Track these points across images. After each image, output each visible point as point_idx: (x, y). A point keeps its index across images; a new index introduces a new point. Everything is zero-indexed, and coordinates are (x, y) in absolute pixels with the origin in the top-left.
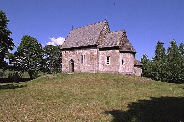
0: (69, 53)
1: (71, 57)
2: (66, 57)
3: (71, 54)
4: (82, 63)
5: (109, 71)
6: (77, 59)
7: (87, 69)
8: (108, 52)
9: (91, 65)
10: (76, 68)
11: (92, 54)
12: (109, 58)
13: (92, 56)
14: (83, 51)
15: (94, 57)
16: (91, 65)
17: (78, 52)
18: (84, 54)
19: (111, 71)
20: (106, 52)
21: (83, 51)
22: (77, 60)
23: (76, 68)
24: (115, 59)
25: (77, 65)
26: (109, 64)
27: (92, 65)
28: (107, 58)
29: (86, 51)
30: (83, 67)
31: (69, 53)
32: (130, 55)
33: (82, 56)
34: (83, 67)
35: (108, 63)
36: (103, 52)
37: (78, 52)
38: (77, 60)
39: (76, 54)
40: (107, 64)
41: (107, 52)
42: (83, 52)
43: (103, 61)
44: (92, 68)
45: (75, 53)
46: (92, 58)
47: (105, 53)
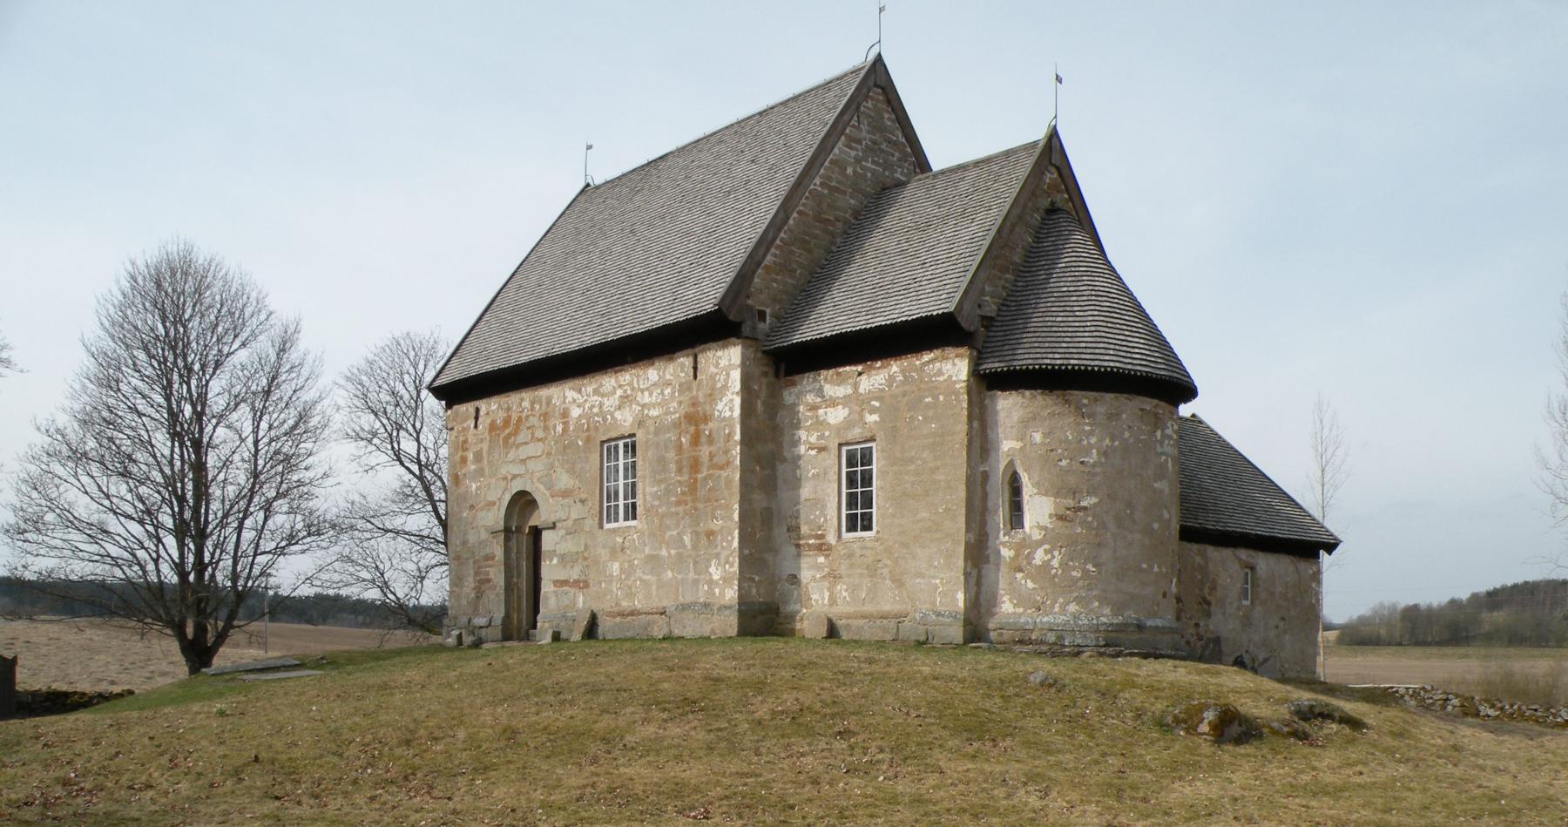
3: (521, 438)
5: (868, 608)
6: (564, 480)
8: (856, 386)
9: (687, 539)
12: (866, 458)
13: (696, 441)
15: (711, 456)
16: (687, 539)
18: (625, 419)
19: (886, 607)
21: (619, 392)
24: (935, 470)
25: (569, 546)
27: (695, 547)
29: (647, 399)
30: (616, 566)
31: (507, 422)
32: (1101, 409)
34: (615, 567)
37: (575, 412)
38: (565, 494)
39: (559, 428)
41: (849, 391)
44: (696, 582)
45: (551, 423)
46: (695, 466)
47: (833, 403)
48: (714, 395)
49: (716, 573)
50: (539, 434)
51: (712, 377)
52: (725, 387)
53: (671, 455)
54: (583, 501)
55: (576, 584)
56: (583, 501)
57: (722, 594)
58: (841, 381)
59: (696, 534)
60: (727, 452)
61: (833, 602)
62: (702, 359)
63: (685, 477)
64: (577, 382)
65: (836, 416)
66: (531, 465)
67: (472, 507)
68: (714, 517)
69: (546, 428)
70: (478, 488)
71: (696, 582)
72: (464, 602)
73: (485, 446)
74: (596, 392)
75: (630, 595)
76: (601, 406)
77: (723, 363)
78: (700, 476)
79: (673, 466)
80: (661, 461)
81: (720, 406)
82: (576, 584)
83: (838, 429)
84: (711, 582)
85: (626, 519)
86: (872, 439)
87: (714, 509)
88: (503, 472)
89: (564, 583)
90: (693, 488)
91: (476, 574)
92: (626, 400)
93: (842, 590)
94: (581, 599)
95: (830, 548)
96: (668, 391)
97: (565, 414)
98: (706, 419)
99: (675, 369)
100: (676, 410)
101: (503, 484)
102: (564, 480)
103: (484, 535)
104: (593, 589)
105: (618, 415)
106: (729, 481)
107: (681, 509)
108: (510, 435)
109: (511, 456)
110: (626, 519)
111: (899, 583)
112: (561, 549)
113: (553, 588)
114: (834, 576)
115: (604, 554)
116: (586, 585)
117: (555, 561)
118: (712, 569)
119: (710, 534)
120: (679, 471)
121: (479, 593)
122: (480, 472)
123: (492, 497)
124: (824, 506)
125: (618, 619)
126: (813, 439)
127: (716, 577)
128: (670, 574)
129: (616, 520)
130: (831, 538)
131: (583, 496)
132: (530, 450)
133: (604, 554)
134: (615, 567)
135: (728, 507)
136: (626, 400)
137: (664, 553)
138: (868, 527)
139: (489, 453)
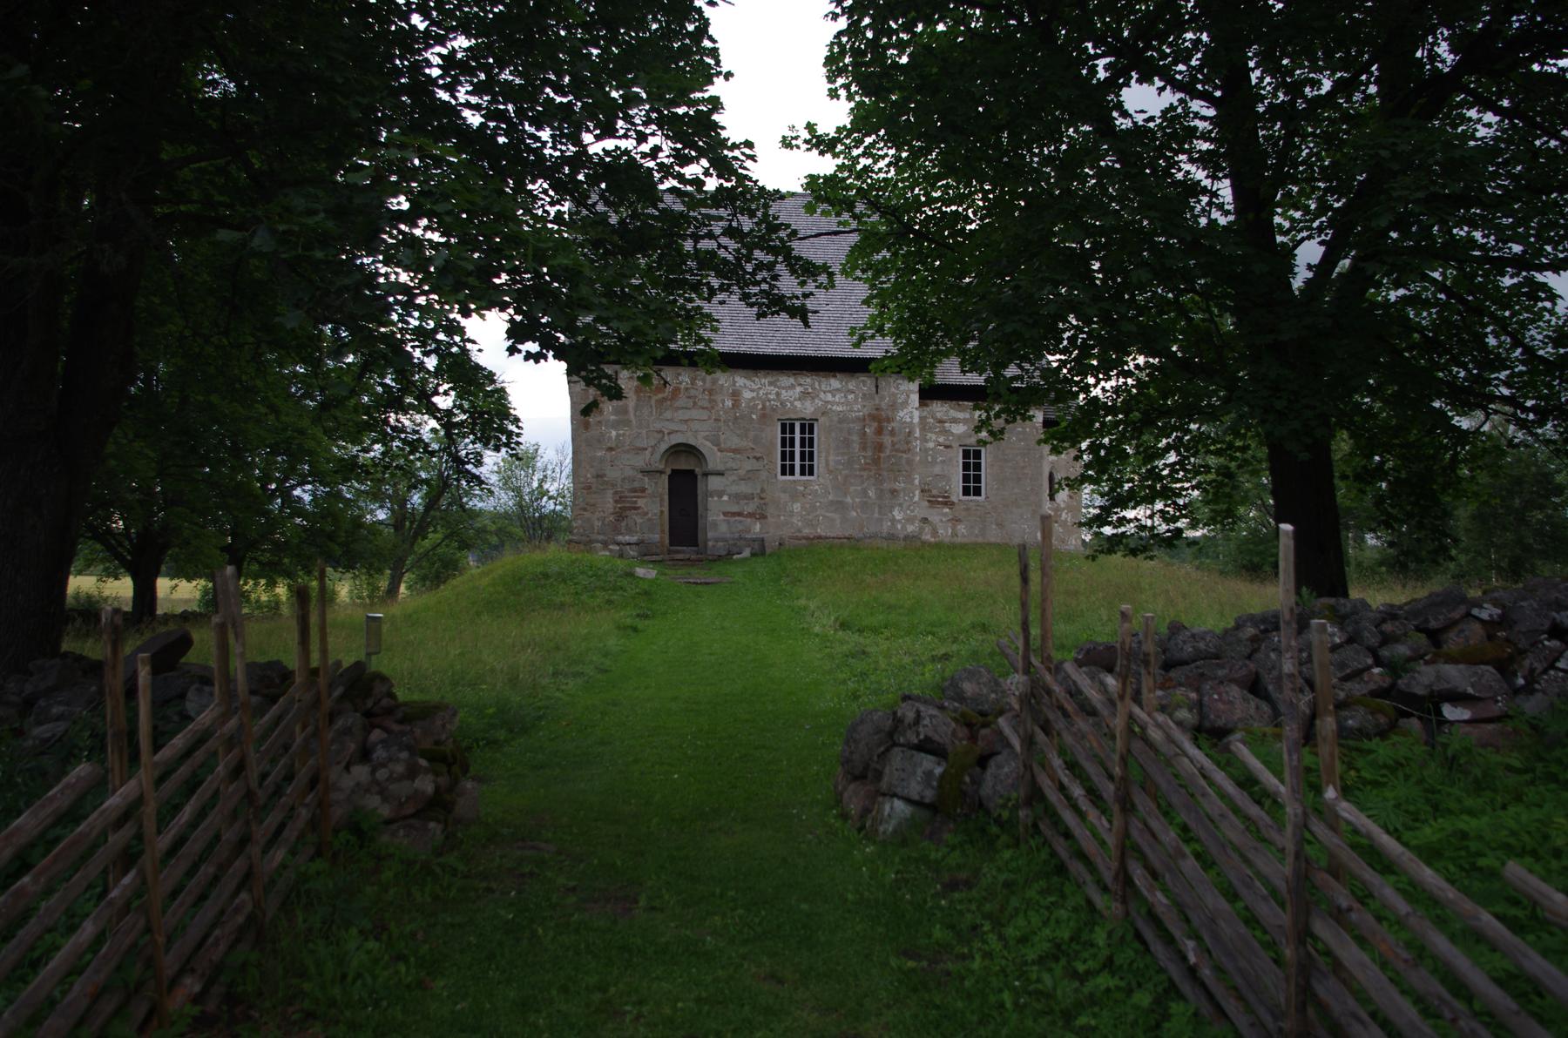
2: (627, 423)
3: (678, 403)
4: (788, 477)
5: (980, 540)
6: (735, 442)
7: (830, 525)
10: (725, 514)
11: (880, 420)
12: (978, 454)
13: (879, 431)
14: (799, 389)
15: (893, 444)
17: (751, 388)
18: (807, 409)
20: (961, 415)
21: (799, 389)
22: (735, 451)
23: (725, 514)
25: (744, 488)
26: (977, 492)
28: (966, 454)
29: (829, 397)
33: (788, 428)
34: (797, 507)
35: (972, 485)
36: (939, 415)
37: (747, 395)
38: (735, 451)
39: (729, 403)
40: (966, 492)
42: (794, 395)
43: (937, 470)
44: (880, 520)
45: (719, 398)
46: (880, 447)
47: (955, 421)
48: (894, 406)
49: (898, 514)
51: (894, 395)
52: (905, 403)
53: (855, 438)
54: (757, 459)
55: (751, 515)
56: (757, 459)
57: (904, 528)
58: (963, 411)
60: (908, 443)
61: (955, 534)
62: (882, 384)
63: (869, 454)
64: (750, 373)
65: (959, 429)
66: (695, 426)
67: (611, 449)
68: (896, 480)
69: (711, 401)
70: (618, 436)
74: (771, 384)
76: (778, 394)
77: (902, 388)
79: (856, 446)
80: (847, 443)
81: (901, 414)
82: (751, 515)
83: (959, 437)
84: (893, 520)
85: (803, 473)
88: (658, 426)
89: (739, 514)
93: (961, 528)
94: (758, 527)
95: (953, 503)
96: (851, 397)
97: (736, 395)
98: (889, 420)
99: (860, 385)
100: (859, 409)
105: (798, 404)
107: (865, 474)
108: (665, 399)
109: (668, 415)
110: (803, 473)
111: (1000, 525)
112: (734, 489)
114: (956, 520)
116: (763, 517)
117: (725, 498)
119: (894, 492)
120: (864, 449)
121: (621, 515)
122: (627, 423)
124: (949, 480)
126: (941, 440)
129: (792, 473)
130: (954, 499)
132: (695, 414)
137: (849, 500)
138: (977, 492)
139: (636, 408)
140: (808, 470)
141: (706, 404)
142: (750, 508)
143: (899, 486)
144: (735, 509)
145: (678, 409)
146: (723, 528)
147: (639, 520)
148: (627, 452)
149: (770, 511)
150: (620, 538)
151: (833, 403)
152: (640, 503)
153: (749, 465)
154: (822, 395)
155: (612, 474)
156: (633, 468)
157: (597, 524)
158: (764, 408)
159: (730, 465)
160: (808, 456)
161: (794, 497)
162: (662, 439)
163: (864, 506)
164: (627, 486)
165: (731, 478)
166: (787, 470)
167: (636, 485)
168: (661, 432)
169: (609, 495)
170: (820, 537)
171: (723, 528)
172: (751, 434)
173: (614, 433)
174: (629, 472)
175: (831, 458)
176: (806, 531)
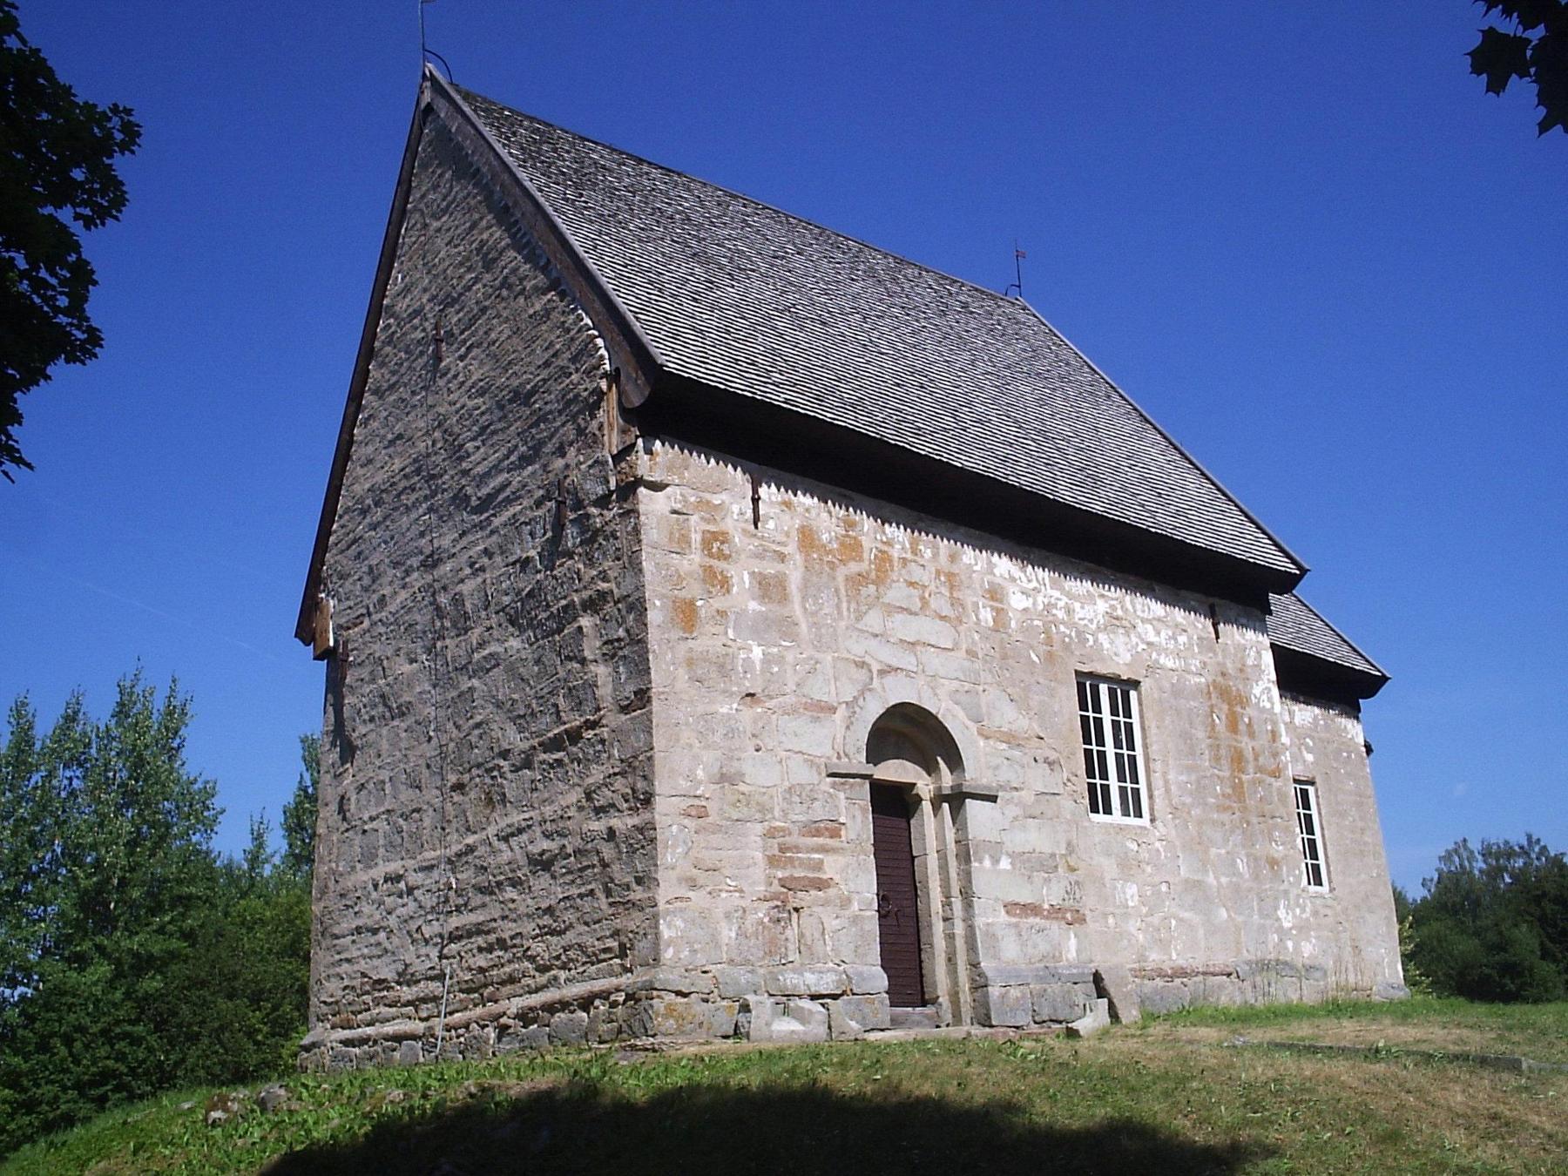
0: (851, 548)
1: (907, 661)
2: (786, 628)
4: (1100, 818)
6: (1008, 717)
13: (1233, 726)
14: (1102, 606)
23: (1010, 907)
25: (1035, 838)
27: (1256, 877)
30: (1132, 890)
34: (1131, 893)
37: (1017, 602)
38: (1011, 739)
39: (987, 616)
44: (1262, 929)
46: (1238, 759)
49: (1286, 919)
50: (940, 604)
53: (1200, 734)
55: (1056, 912)
59: (1254, 860)
60: (1275, 755)
63: (1227, 774)
69: (955, 602)
70: (767, 660)
71: (1262, 929)
72: (728, 933)
73: (795, 575)
75: (1164, 945)
76: (1069, 611)
78: (1244, 777)
82: (1056, 912)
84: (1280, 930)
86: (1312, 783)
87: (1275, 827)
89: (1032, 909)
90: (1238, 788)
91: (772, 861)
92: (1114, 622)
96: (1182, 639)
97: (995, 594)
101: (862, 675)
102: (1008, 717)
103: (803, 775)
104: (1092, 925)
106: (1283, 797)
107: (1225, 817)
109: (873, 620)
113: (1003, 917)
115: (1109, 867)
116: (1079, 919)
117: (1005, 864)
118: (1281, 913)
119: (1273, 863)
122: (786, 628)
123: (820, 690)
125: (1159, 982)
127: (1287, 925)
128: (1223, 913)
129: (1108, 810)
131: (1053, 756)
133: (1109, 867)
134: (1131, 893)
135: (1287, 830)
136: (1114, 622)
137: (1211, 879)
140: (1132, 804)
141: (947, 610)
142: (1052, 895)
143: (1278, 850)
144: (1025, 897)
145: (892, 610)
146: (1010, 950)
147: (832, 924)
148: (791, 711)
149: (1089, 903)
150: (790, 980)
151: (1161, 650)
152: (832, 867)
153: (1039, 779)
154: (1140, 628)
155: (760, 774)
156: (811, 762)
157: (728, 933)
158: (1049, 642)
159: (1007, 775)
160: (1128, 768)
161: (1128, 867)
162: (866, 689)
163: (1236, 895)
164: (799, 816)
165: (1012, 811)
166: (1098, 801)
167: (819, 812)
168: (862, 665)
169: (754, 849)
170: (1182, 973)
171: (1010, 950)
172: (1035, 700)
173: (757, 653)
174: (803, 775)
175: (1171, 777)
176: (1154, 958)
